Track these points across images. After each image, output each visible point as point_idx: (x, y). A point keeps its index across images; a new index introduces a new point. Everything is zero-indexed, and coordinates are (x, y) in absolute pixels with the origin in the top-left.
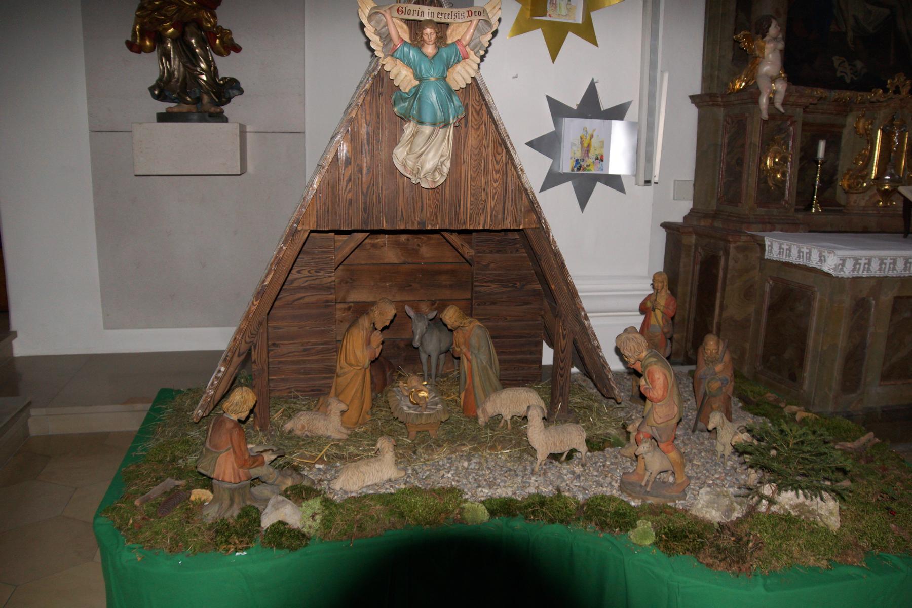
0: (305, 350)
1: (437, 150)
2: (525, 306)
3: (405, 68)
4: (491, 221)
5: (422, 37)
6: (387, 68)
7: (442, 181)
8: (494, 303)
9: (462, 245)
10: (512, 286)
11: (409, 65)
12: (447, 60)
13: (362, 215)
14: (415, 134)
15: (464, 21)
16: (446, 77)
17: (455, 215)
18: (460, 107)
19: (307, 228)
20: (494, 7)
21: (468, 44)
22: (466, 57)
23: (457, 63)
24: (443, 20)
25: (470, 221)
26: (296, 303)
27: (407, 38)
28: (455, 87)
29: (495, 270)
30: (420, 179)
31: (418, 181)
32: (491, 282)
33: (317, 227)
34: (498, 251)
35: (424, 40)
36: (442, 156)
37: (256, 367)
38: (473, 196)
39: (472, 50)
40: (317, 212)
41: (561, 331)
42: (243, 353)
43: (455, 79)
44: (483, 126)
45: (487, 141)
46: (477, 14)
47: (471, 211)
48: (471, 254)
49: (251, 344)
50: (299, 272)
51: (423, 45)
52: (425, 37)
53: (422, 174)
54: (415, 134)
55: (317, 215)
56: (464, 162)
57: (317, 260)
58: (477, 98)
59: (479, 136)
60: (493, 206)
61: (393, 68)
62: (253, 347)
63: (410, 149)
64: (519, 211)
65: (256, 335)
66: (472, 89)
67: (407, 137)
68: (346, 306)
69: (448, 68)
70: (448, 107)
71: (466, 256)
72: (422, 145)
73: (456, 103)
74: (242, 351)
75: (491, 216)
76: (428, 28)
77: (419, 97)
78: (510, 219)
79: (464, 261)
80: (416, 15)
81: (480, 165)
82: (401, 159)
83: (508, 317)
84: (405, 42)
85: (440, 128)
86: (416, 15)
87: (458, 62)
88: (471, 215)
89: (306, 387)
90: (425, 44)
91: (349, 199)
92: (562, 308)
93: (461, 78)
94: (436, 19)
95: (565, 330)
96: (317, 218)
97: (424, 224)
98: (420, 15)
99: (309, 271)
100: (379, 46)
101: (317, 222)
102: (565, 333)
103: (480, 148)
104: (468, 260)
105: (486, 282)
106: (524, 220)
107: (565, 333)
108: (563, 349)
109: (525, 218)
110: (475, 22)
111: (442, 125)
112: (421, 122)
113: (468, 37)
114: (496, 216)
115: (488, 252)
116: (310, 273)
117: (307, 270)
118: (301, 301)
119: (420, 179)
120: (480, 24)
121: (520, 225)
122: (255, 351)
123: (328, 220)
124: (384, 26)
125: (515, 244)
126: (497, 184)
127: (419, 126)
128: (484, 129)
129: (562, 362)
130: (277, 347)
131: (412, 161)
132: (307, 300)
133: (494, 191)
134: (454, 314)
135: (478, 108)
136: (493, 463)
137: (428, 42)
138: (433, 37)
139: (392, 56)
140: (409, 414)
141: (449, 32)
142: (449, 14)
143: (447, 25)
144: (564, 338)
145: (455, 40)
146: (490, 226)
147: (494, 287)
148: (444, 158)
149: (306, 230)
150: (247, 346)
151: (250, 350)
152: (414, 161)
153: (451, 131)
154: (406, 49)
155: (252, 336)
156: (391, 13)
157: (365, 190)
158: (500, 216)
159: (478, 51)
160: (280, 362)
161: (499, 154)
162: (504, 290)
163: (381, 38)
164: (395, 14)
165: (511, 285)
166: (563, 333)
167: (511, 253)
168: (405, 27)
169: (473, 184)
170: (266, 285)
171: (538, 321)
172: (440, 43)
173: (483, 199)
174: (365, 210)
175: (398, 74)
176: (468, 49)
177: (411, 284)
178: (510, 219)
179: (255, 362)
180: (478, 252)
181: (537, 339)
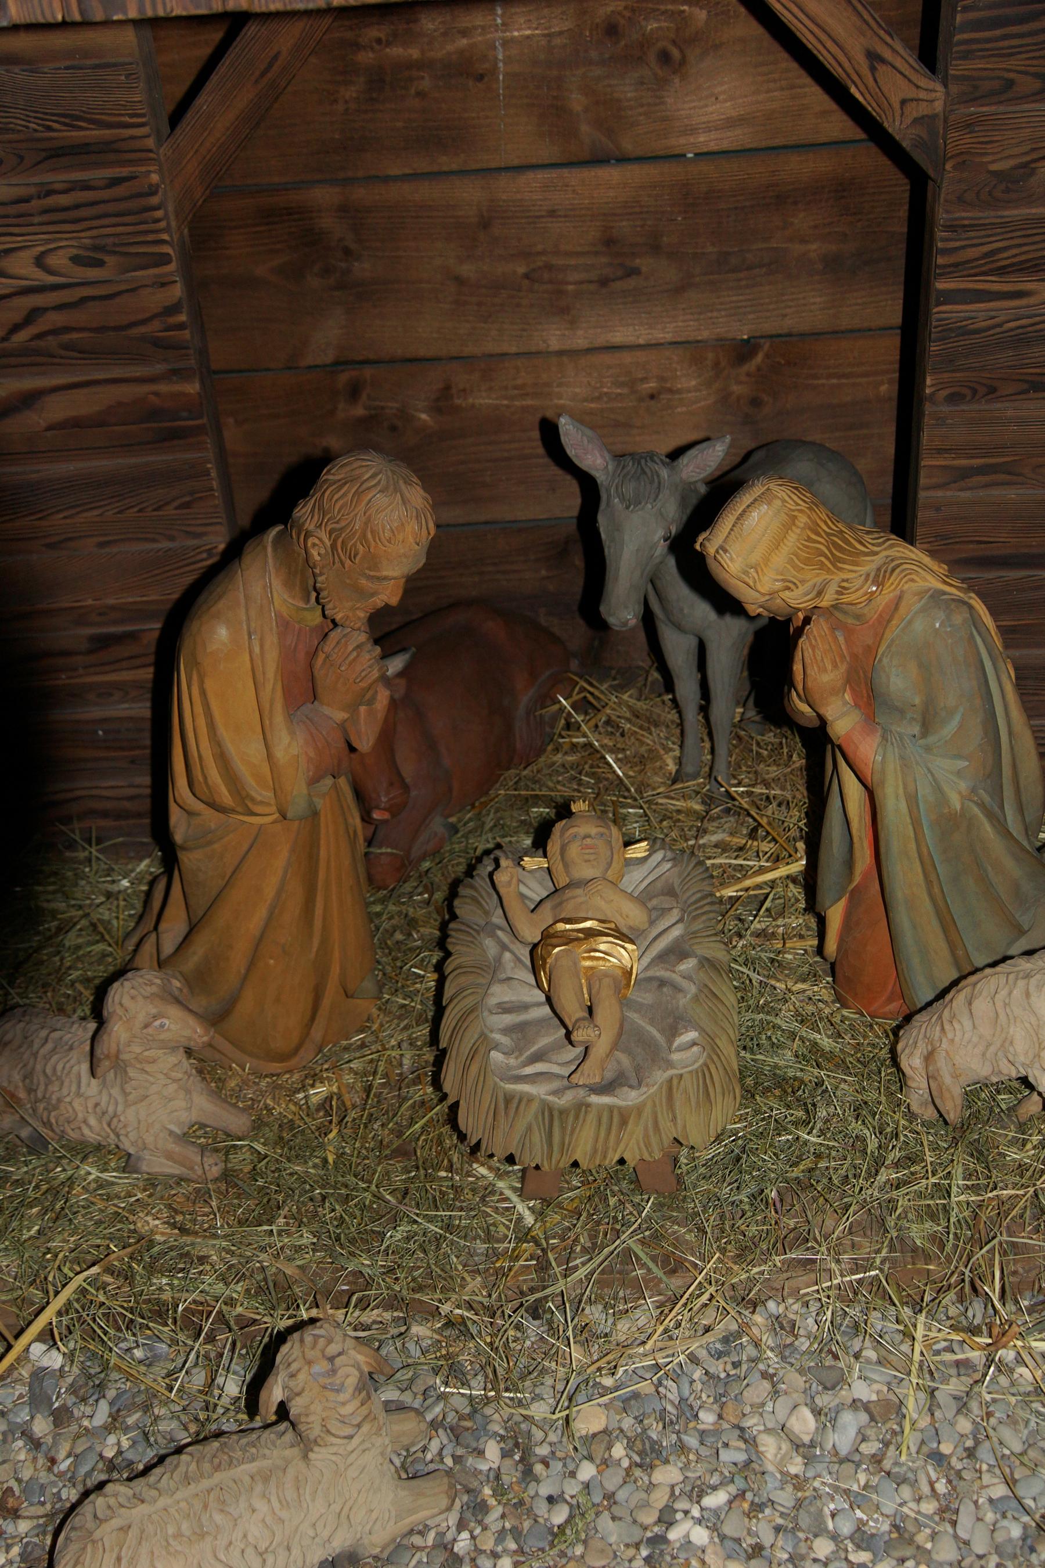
9: (874, 58)
48: (923, 109)
57: (63, 200)
71: (896, 126)
89: (131, 798)
99: (39, 262)
105: (1001, 271)
116: (51, 272)
117: (27, 256)
134: (777, 544)
136: (964, 1425)
140: (508, 1099)
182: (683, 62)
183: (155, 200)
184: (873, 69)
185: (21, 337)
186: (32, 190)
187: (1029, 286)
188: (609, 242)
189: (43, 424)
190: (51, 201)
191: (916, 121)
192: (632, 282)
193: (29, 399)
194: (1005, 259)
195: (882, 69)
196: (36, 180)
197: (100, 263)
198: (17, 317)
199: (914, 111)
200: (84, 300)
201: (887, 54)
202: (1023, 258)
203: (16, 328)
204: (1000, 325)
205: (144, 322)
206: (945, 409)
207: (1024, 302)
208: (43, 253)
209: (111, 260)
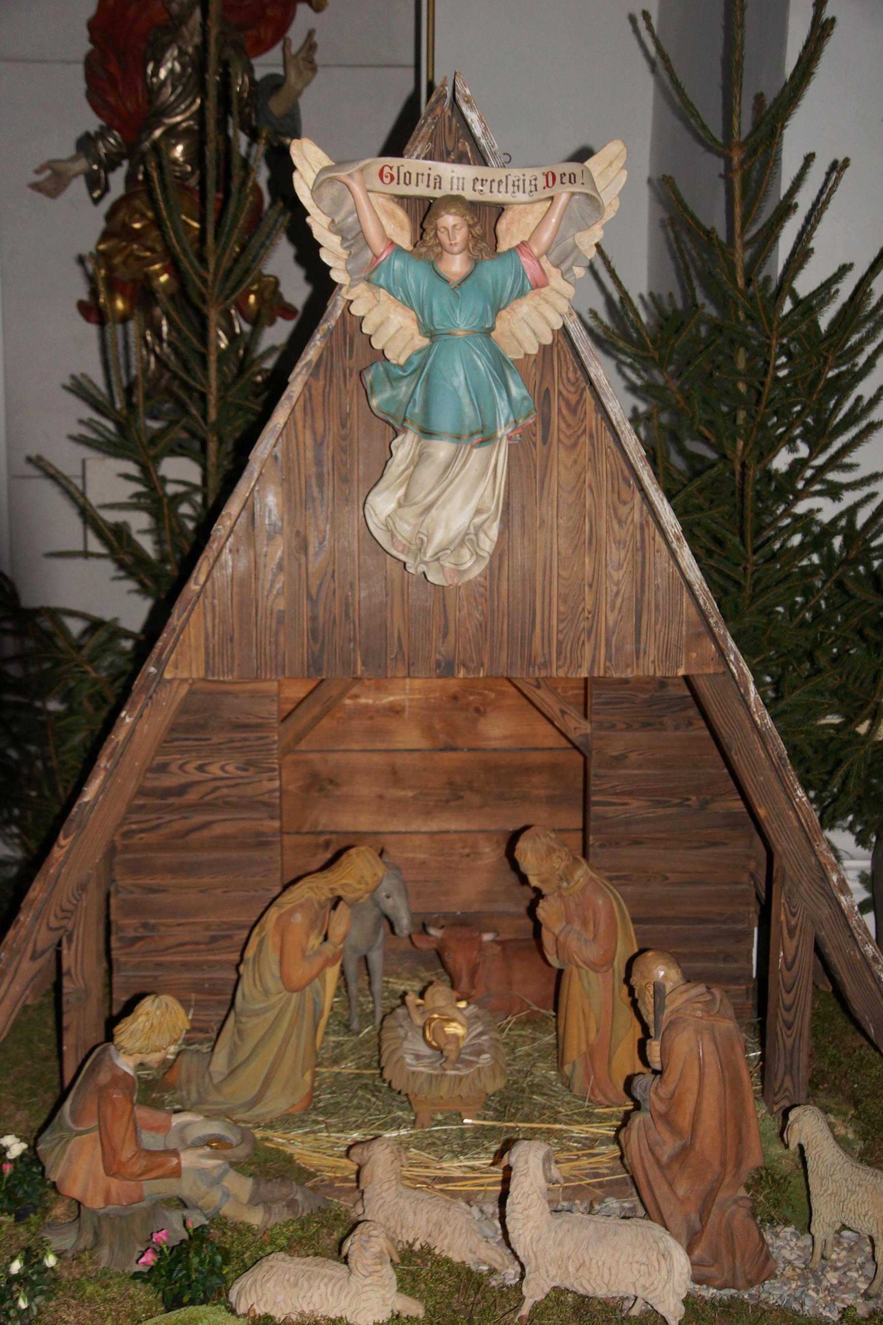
0: (214, 939)
1: (468, 498)
2: (710, 850)
3: (399, 309)
4: (608, 658)
5: (436, 235)
6: (357, 310)
7: (476, 571)
8: (636, 842)
9: (563, 712)
10: (680, 805)
11: (407, 302)
12: (495, 291)
13: (308, 645)
14: (419, 459)
15: (536, 196)
16: (492, 329)
17: (522, 644)
18: (524, 398)
19: (185, 675)
20: (611, 164)
21: (546, 253)
22: (540, 284)
23: (518, 297)
24: (487, 197)
25: (558, 659)
26: (194, 836)
27: (404, 240)
28: (513, 354)
29: (640, 767)
30: (426, 563)
31: (422, 568)
32: (630, 793)
33: (206, 673)
34: (645, 725)
35: (440, 244)
36: (478, 512)
37: (72, 986)
38: (565, 601)
39: (557, 266)
40: (207, 638)
41: (783, 918)
42: (43, 952)
43: (513, 335)
44: (585, 439)
45: (596, 472)
46: (566, 179)
47: (561, 637)
48: (583, 732)
49: (62, 931)
50: (201, 768)
51: (439, 256)
52: (443, 237)
53: (430, 552)
54: (419, 459)
55: (206, 648)
56: (543, 522)
58: (571, 375)
59: (575, 462)
60: (611, 623)
61: (370, 310)
62: (64, 939)
63: (406, 495)
64: (673, 635)
66: (559, 353)
67: (398, 466)
68: (322, 839)
69: (497, 310)
70: (494, 400)
71: (572, 736)
72: (430, 487)
73: (516, 391)
74: (40, 947)
75: (608, 645)
76: (448, 213)
77: (428, 375)
78: (652, 652)
79: (570, 746)
80: (422, 186)
81: (580, 529)
82: (382, 517)
83: (668, 875)
84: (398, 250)
85: (473, 447)
86: (422, 186)
87: (522, 294)
88: (560, 643)
90: (445, 253)
91: (280, 611)
92: (784, 861)
93: (529, 333)
94: (469, 195)
95: (794, 915)
96: (207, 653)
98: (432, 184)
99: (222, 768)
100: (338, 258)
101: (207, 663)
102: (793, 923)
103: (581, 490)
104: (577, 744)
105: (617, 794)
106: (688, 656)
107: (793, 923)
108: (790, 958)
109: (689, 651)
110: (563, 199)
111: (477, 438)
112: (427, 433)
113: (546, 236)
114: (619, 649)
115: (624, 726)
116: (225, 771)
117: (218, 765)
118: (206, 833)
119: (426, 563)
120: (574, 205)
121: (678, 667)
122: (69, 948)
123: (233, 657)
124: (350, 213)
125: (685, 709)
126: (622, 572)
127: (424, 442)
128: (588, 447)
129: (788, 992)
131: (409, 524)
132: (218, 830)
133: (615, 589)
135: (573, 398)
137: (448, 247)
138: (460, 236)
139: (368, 281)
141: (502, 226)
142: (500, 182)
143: (500, 209)
144: (792, 933)
145: (515, 243)
146: (606, 669)
147: (636, 805)
148: (483, 517)
149: (183, 681)
150: (54, 937)
151: (60, 944)
152: (413, 521)
153: (501, 455)
154: (397, 264)
155: (65, 914)
156: (363, 183)
157: (314, 590)
158: (629, 648)
159: (570, 269)
160: (159, 965)
161: (625, 503)
162: (660, 812)
163: (344, 239)
164: (377, 184)
165: (677, 801)
166: (788, 922)
167: (677, 728)
168: (400, 214)
169: (564, 573)
170: (87, 803)
171: (741, 883)
172: (481, 251)
173: (589, 607)
174: (314, 634)
175: (382, 323)
176: (547, 265)
178: (652, 652)
179: (69, 973)
180: (600, 726)
181: (740, 927)
182: (485, 712)
187: (629, 801)
188: (451, 784)
191: (581, 736)
192: (460, 802)
194: (619, 789)
199: (579, 732)
206: (598, 850)
209: (252, 769)
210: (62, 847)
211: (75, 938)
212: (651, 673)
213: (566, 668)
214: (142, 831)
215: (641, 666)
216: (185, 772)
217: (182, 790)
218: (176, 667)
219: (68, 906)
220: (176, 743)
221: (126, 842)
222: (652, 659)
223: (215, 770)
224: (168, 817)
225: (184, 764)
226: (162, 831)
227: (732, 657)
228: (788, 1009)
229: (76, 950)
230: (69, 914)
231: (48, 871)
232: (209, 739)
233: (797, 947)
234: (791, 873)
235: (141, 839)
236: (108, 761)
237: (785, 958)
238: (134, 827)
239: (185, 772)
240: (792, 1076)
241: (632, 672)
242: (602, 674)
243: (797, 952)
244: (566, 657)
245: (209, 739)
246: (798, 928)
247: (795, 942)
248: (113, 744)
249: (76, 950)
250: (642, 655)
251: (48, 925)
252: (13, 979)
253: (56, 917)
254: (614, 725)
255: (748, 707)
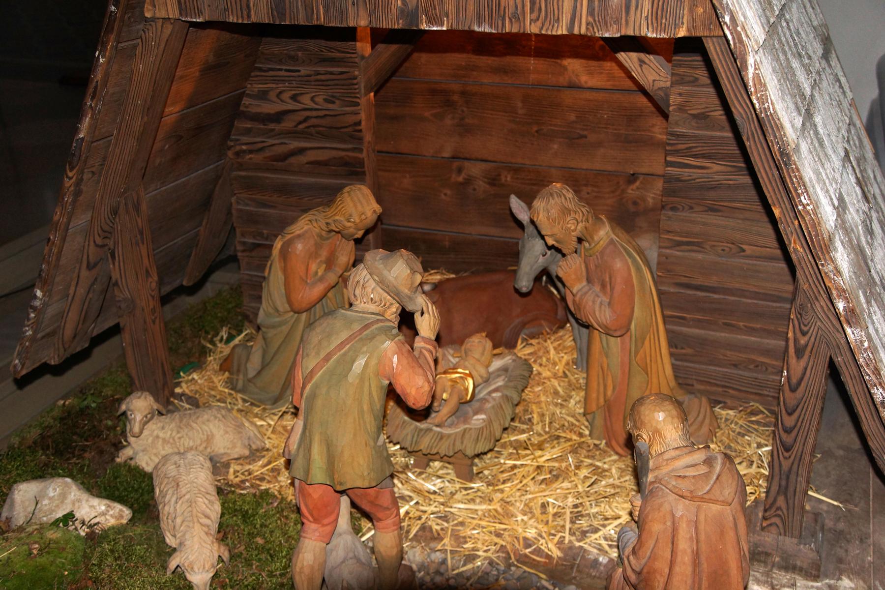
4: (591, 12)
25: (532, 10)
26: (292, 160)
50: (294, 98)
65: (110, 233)
83: (744, 247)
97: (413, 16)
99: (312, 99)
102: (803, 341)
105: (695, 156)
108: (794, 381)
116: (316, 104)
117: (309, 96)
118: (303, 159)
122: (114, 264)
130: (267, 239)
132: (311, 156)
144: (799, 353)
155: (107, 234)
166: (796, 340)
177: (585, 133)
183: (355, 81)
184: (641, 66)
185: (301, 126)
186: (313, 73)
189: (305, 161)
190: (319, 77)
193: (301, 151)
195: (644, 66)
196: (314, 69)
197: (333, 103)
198: (301, 119)
200: (326, 115)
201: (646, 61)
202: (704, 152)
203: (300, 123)
204: (694, 180)
205: (346, 127)
207: (705, 171)
208: (314, 96)
209: (337, 102)
210: (70, 178)
211: (117, 256)
212: (643, 34)
213: (539, 23)
214: (251, 152)
215: (631, 24)
216: (282, 101)
217: (278, 117)
218: (154, 6)
219: (106, 228)
220: (271, 73)
221: (239, 160)
222: (645, 14)
223: (306, 100)
224: (271, 141)
225: (281, 93)
226: (268, 153)
227: (727, 19)
228: (788, 431)
229: (120, 267)
230: (109, 235)
231: (63, 199)
232: (299, 71)
233: (806, 369)
234: (806, 287)
235: (250, 159)
236: (92, 100)
237: (789, 378)
238: (244, 147)
239: (282, 101)
240: (786, 497)
241: (619, 30)
242: (583, 31)
243: (804, 374)
244: (540, 9)
245: (299, 71)
246: (809, 349)
247: (803, 363)
248: (94, 84)
249: (120, 267)
250: (633, 9)
251: (95, 242)
252: (77, 283)
253: (99, 236)
254: (697, 79)
255: (745, 86)
